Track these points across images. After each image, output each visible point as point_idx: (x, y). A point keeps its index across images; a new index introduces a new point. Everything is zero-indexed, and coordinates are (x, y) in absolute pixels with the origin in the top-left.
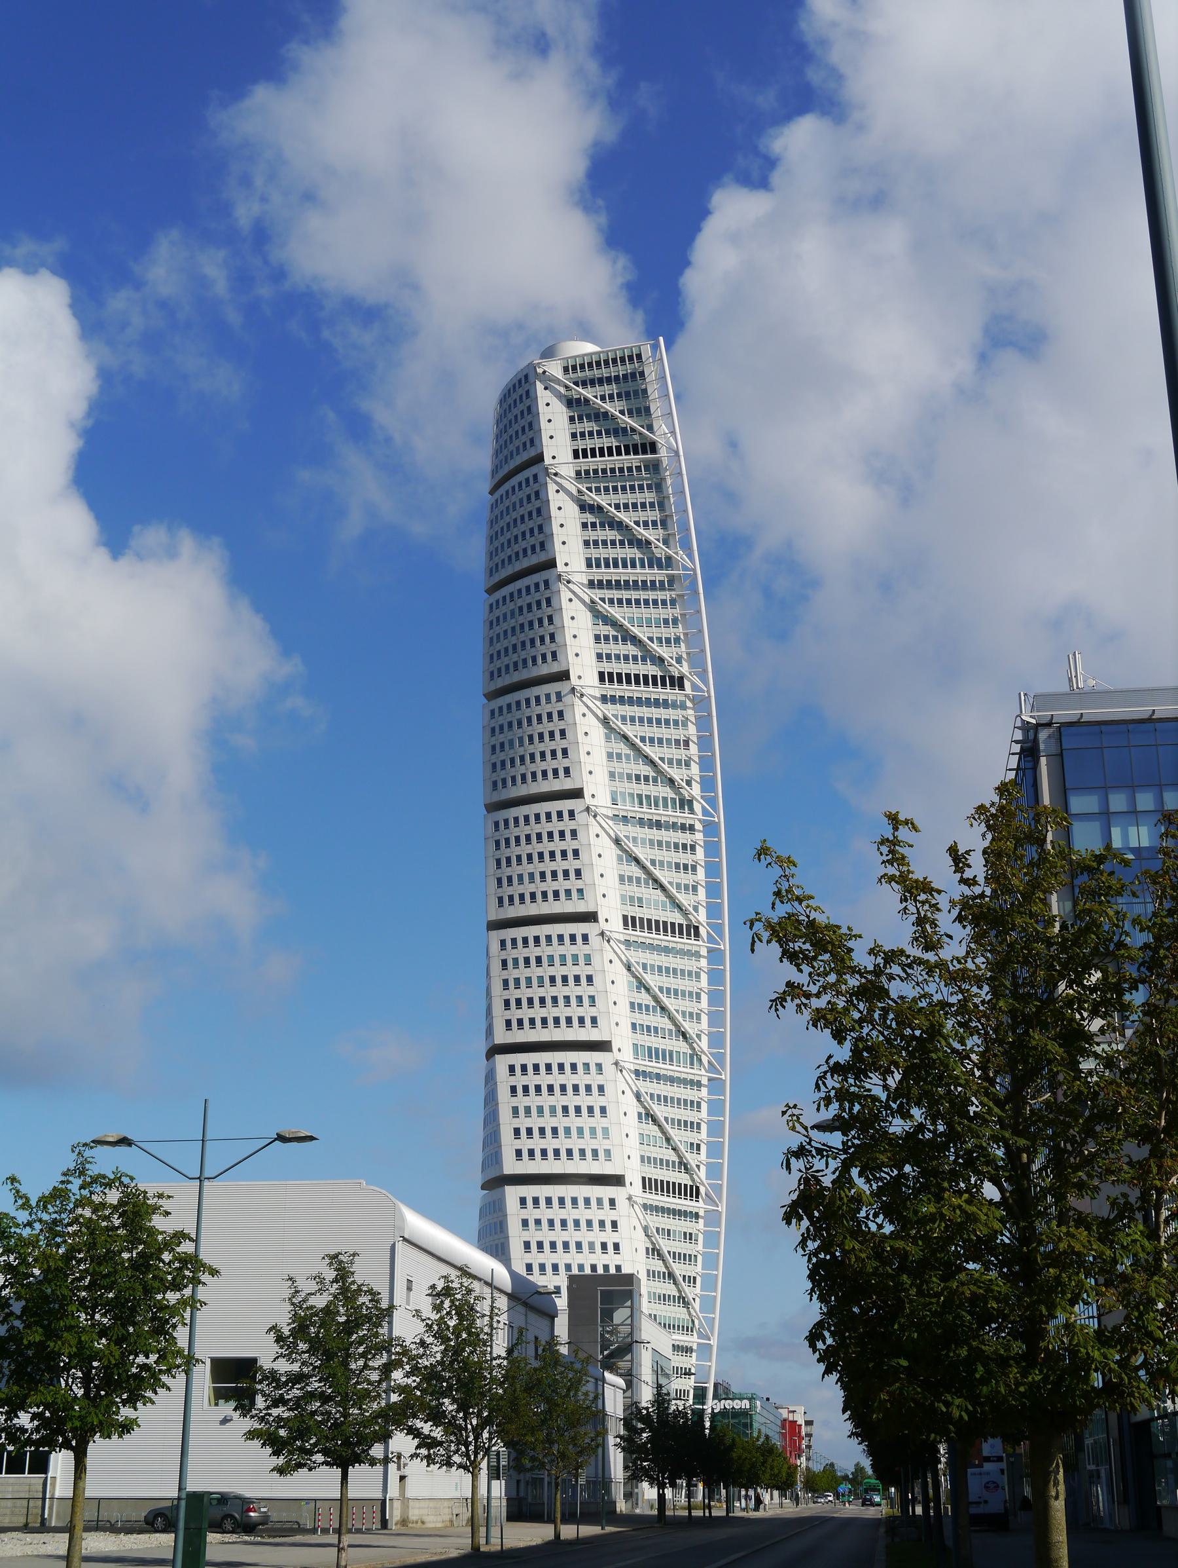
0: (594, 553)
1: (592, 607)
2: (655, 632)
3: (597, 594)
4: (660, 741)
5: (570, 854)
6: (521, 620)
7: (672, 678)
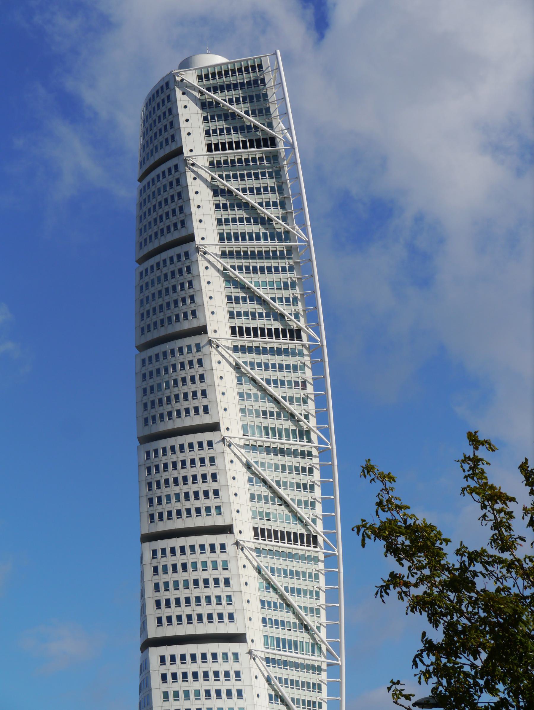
0: (226, 229)
1: (225, 273)
2: (277, 293)
3: (228, 263)
4: (282, 382)
5: (209, 478)
6: (166, 284)
7: (291, 331)
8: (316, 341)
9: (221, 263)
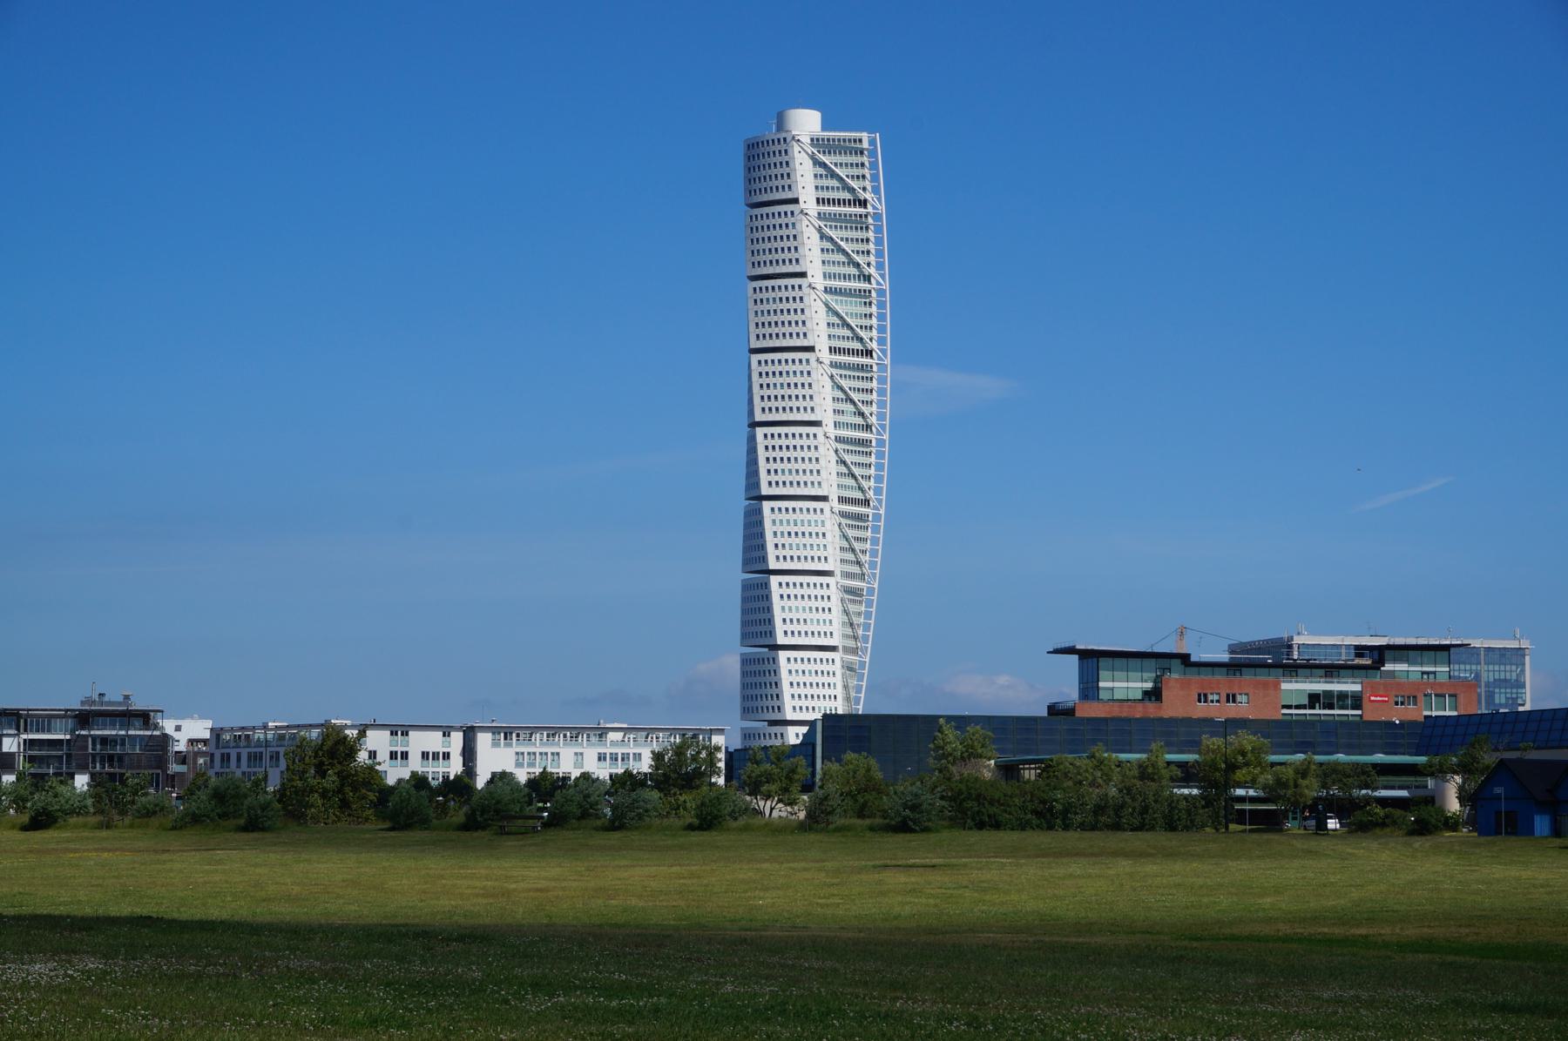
1: (819, 230)
3: (834, 371)
5: (800, 323)
7: (864, 276)
8: (881, 285)
9: (818, 223)
